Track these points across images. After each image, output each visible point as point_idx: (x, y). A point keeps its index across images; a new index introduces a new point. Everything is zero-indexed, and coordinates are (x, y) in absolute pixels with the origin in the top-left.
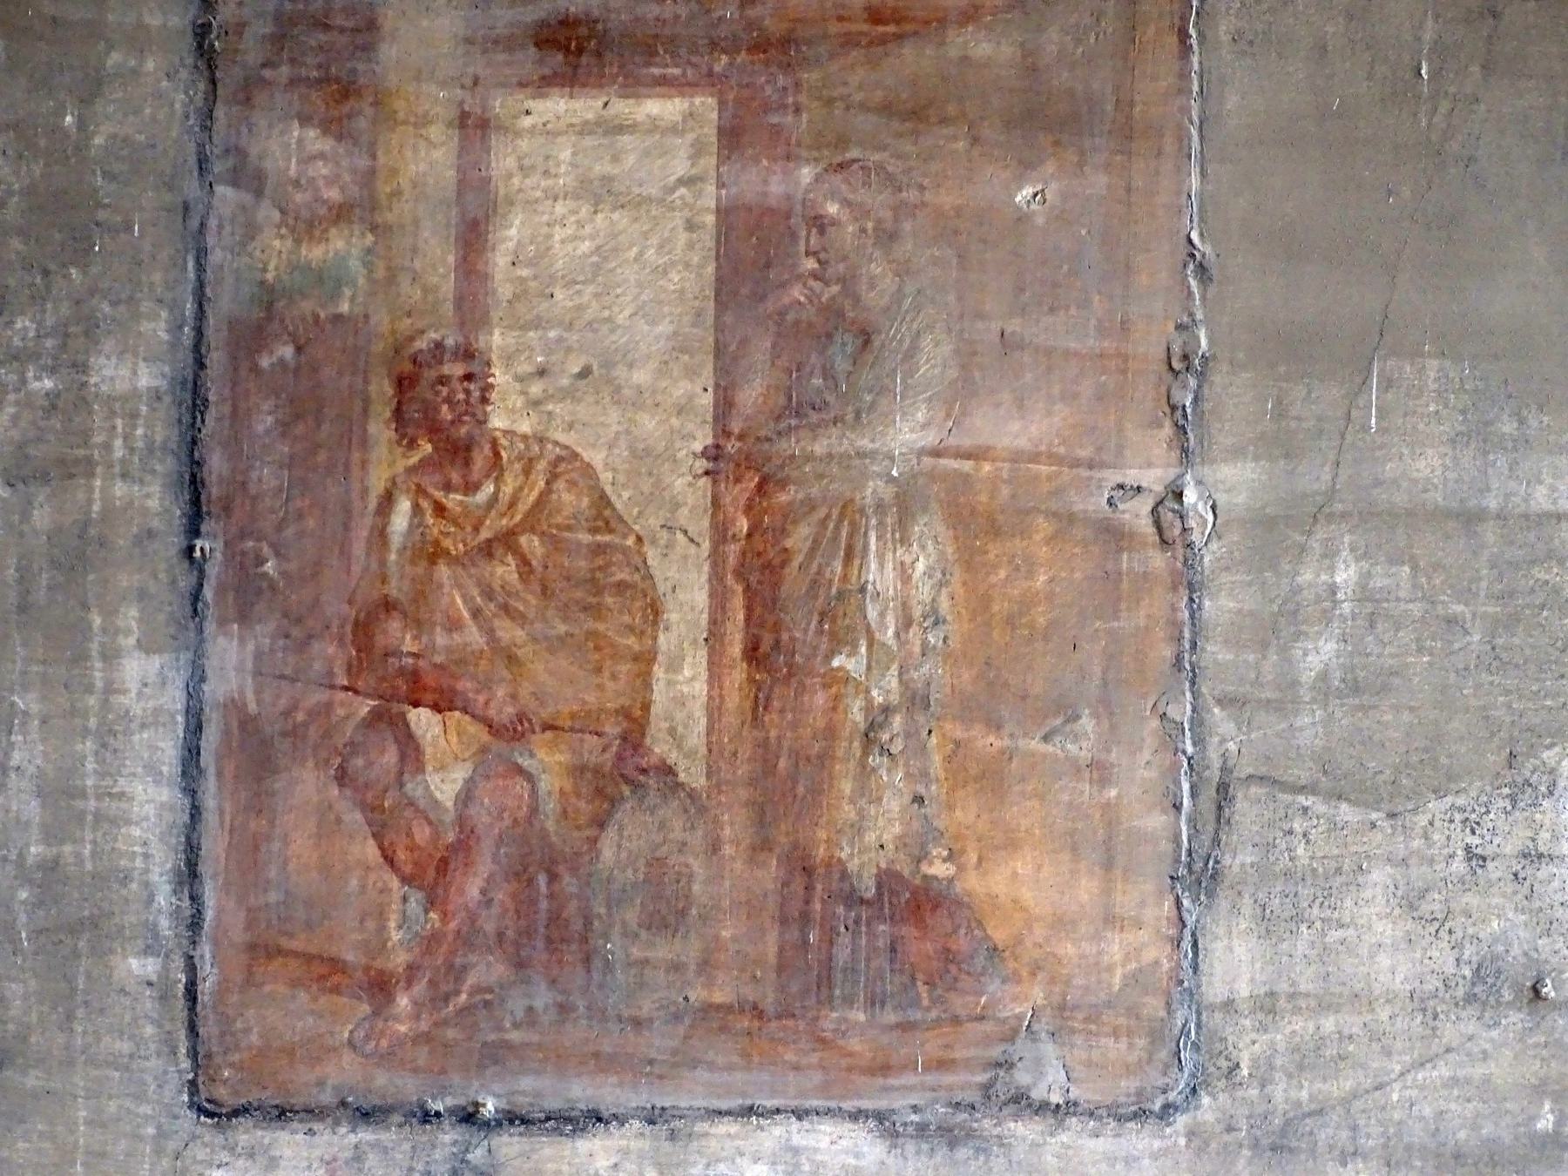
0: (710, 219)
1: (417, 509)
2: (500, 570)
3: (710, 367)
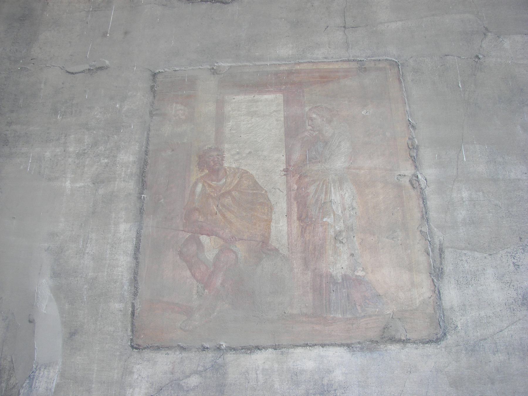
0: (282, 119)
1: (203, 185)
2: (227, 200)
3: (284, 150)
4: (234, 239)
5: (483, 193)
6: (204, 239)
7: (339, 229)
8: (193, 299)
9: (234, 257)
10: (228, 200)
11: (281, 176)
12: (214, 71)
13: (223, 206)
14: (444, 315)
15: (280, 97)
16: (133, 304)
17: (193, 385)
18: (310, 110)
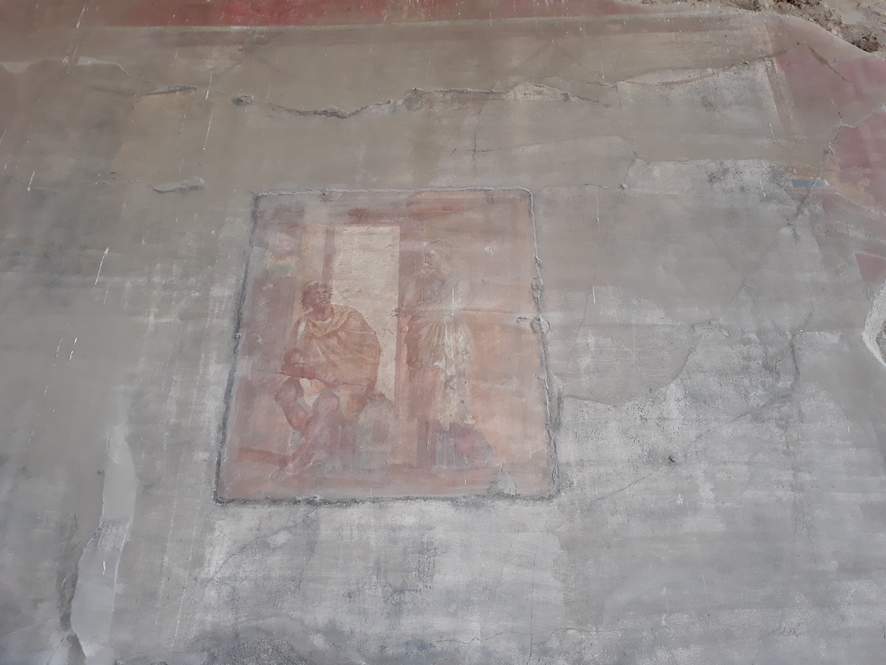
0: (398, 254)
1: (307, 325)
2: (332, 341)
3: (397, 288)
4: (337, 383)
5: (612, 339)
6: (304, 382)
7: (450, 374)
8: (288, 447)
9: (336, 402)
10: (333, 341)
11: (392, 316)
12: (325, 198)
13: (328, 347)
14: (558, 470)
15: (397, 229)
16: (220, 453)
17: (280, 543)
18: (428, 245)
